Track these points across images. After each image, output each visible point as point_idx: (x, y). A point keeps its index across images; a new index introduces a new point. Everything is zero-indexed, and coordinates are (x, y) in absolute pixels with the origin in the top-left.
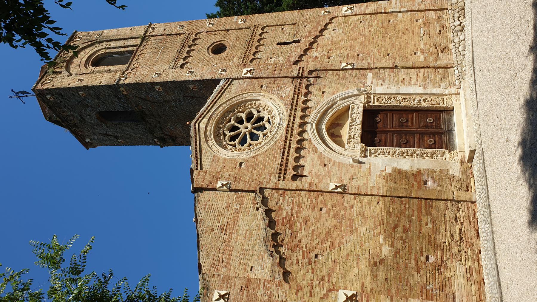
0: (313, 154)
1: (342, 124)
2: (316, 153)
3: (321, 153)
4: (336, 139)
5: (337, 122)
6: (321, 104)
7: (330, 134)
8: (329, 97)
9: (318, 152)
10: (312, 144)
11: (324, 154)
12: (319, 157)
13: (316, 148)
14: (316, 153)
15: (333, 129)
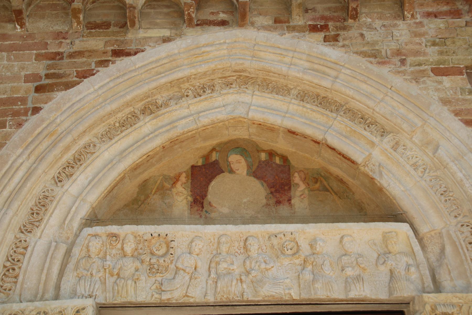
0: (34, 77)
1: (284, 210)
2: (38, 89)
3: (36, 110)
4: (179, 187)
5: (297, 179)
6: (385, 70)
7: (214, 156)
8: (445, 102)
9: (43, 96)
10: (104, 63)
11: (27, 126)
12: (11, 101)
13: (68, 86)
14: (38, 89)
15: (249, 167)
